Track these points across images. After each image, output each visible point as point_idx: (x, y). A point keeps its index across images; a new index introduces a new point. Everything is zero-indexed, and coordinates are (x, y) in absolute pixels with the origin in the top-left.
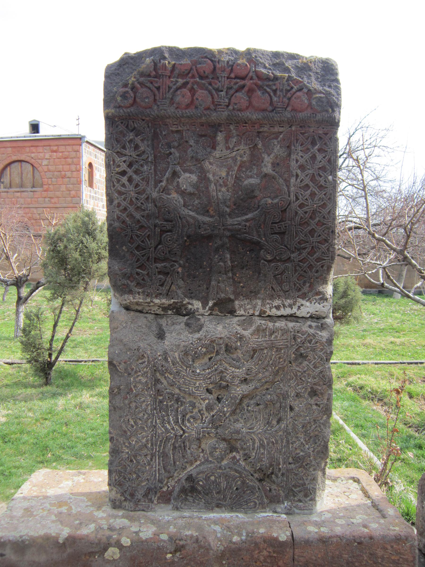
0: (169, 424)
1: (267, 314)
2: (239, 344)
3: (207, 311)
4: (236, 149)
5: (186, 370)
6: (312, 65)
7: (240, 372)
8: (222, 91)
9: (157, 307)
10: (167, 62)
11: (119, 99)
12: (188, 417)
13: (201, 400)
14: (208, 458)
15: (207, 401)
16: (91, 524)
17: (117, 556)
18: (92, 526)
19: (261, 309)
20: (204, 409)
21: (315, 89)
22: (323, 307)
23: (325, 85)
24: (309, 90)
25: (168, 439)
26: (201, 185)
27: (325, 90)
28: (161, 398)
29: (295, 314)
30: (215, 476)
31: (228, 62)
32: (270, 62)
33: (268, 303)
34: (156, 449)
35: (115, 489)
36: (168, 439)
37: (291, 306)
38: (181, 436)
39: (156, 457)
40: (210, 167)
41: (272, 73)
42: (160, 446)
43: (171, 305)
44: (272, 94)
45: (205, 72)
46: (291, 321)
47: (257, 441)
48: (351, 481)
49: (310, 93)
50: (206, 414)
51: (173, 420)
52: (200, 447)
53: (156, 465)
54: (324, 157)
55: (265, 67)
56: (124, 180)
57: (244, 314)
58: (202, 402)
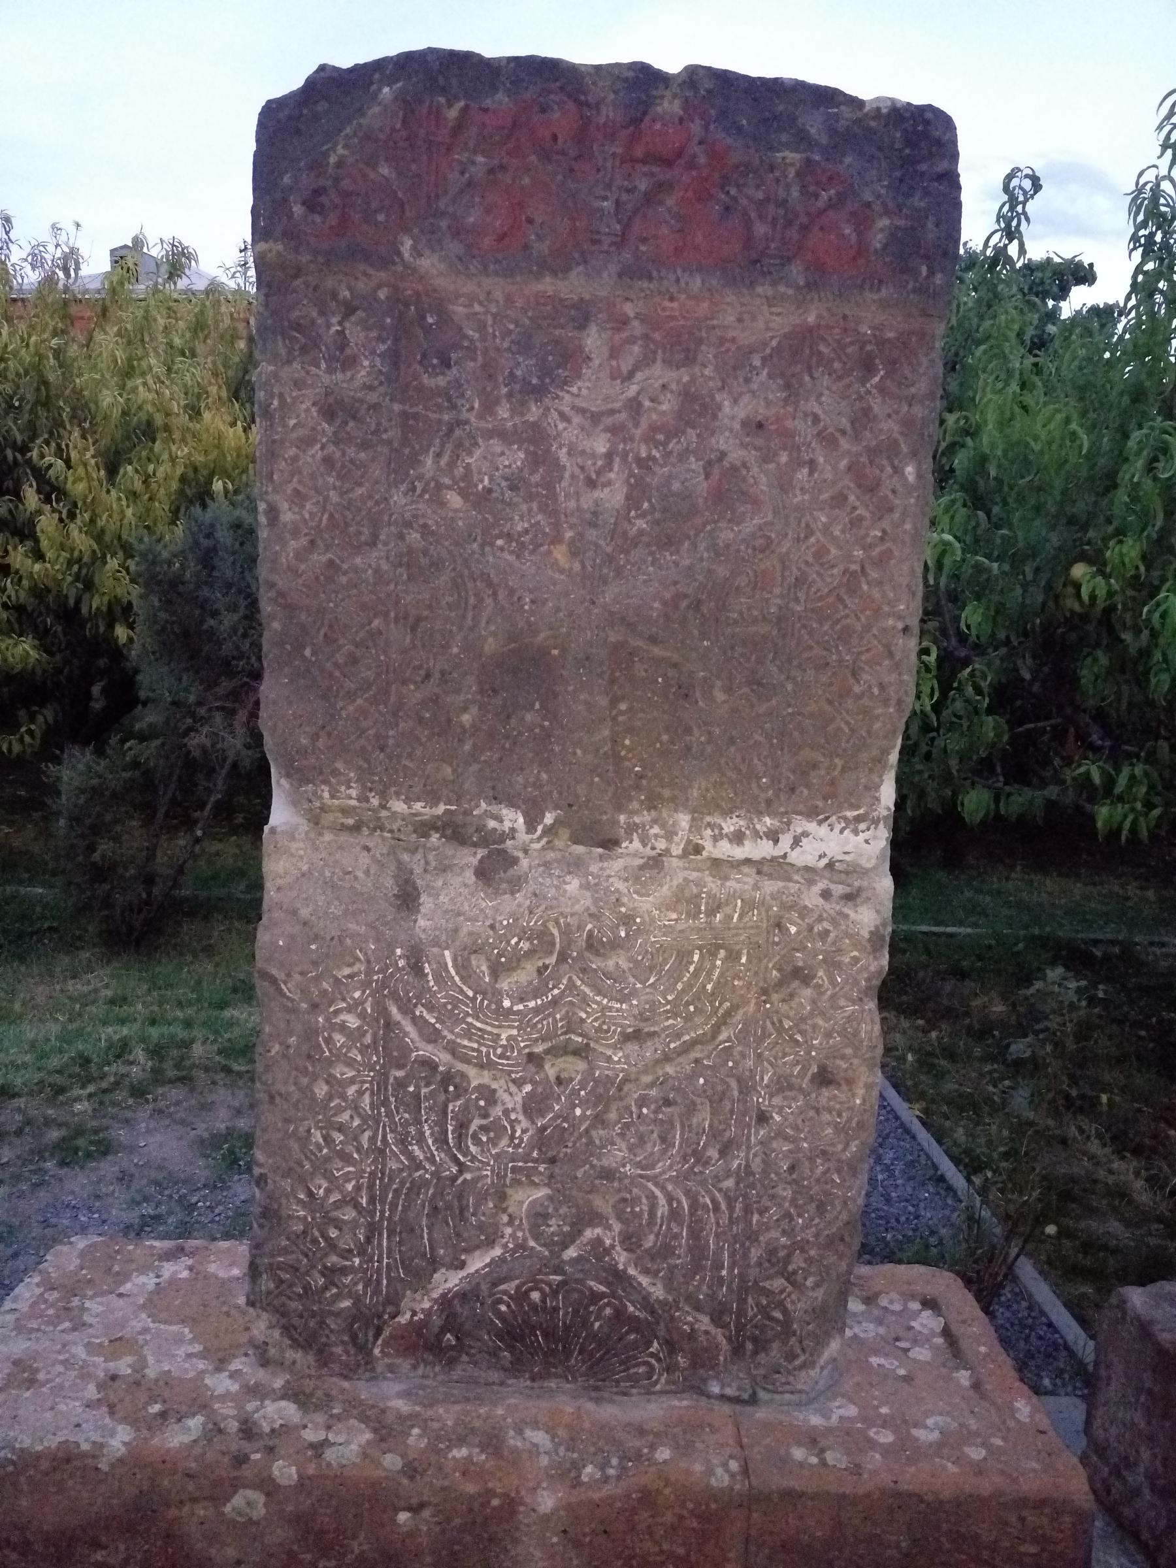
0: (421, 1148)
2: (623, 934)
3: (539, 839)
5: (474, 999)
7: (623, 1013)
9: (400, 822)
11: (298, 210)
12: (473, 1127)
14: (525, 1239)
15: (528, 1088)
16: (194, 1415)
17: (259, 1512)
18: (195, 1423)
19: (689, 842)
20: (519, 1107)
22: (867, 842)
25: (417, 1187)
26: (536, 478)
28: (400, 1074)
29: (785, 856)
30: (541, 1290)
33: (709, 824)
34: (382, 1212)
37: (774, 836)
38: (454, 1179)
39: (380, 1235)
40: (561, 426)
42: (393, 1206)
43: (438, 817)
46: (770, 876)
47: (662, 1201)
50: (525, 1124)
51: (432, 1134)
58: (513, 1089)
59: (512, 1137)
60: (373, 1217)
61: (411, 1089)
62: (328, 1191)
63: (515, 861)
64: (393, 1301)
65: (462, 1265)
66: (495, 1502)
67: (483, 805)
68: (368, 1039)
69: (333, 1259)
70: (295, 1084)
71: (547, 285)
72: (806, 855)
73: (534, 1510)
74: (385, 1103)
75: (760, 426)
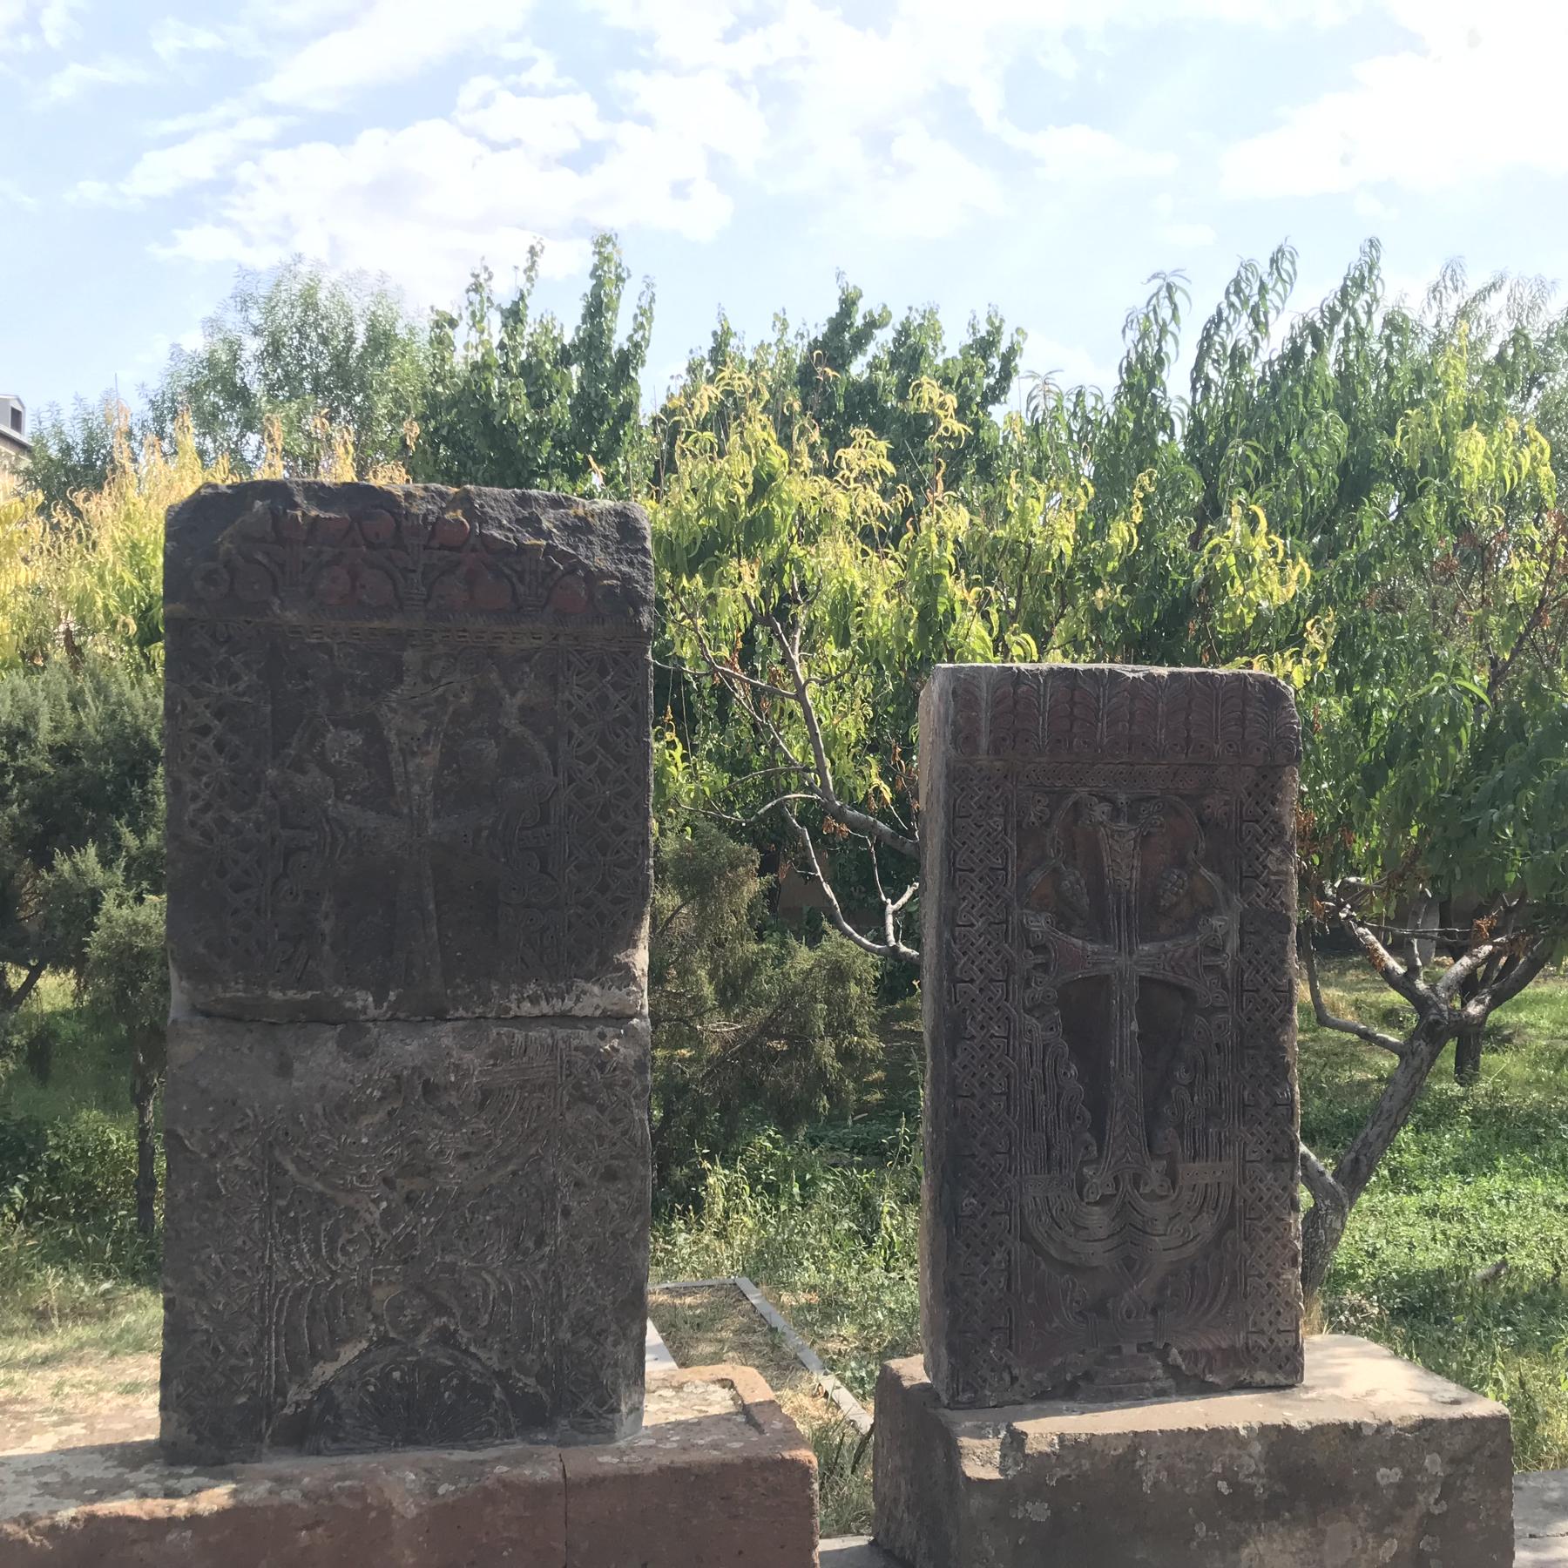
0: (301, 1261)
1: (512, 1013)
2: (453, 1079)
4: (444, 681)
6: (595, 522)
8: (414, 571)
10: (299, 513)
11: (198, 584)
13: (371, 1205)
14: (386, 1332)
21: (601, 570)
23: (621, 561)
24: (588, 572)
25: (299, 1294)
27: (620, 571)
28: (282, 1203)
31: (425, 516)
32: (512, 515)
34: (271, 1318)
35: (175, 1416)
36: (299, 1294)
38: (328, 1284)
39: (270, 1338)
40: (390, 715)
41: (515, 539)
44: (515, 580)
45: (377, 535)
47: (493, 1286)
48: (717, 1387)
49: (592, 577)
52: (368, 1309)
53: (270, 1355)
54: (624, 698)
55: (501, 527)
56: (207, 744)
57: (465, 1015)
58: (372, 1207)
59: (373, 1247)
60: (264, 1323)
61: (292, 1214)
62: (226, 1305)
63: (368, 1031)
64: (281, 1391)
65: (336, 1358)
66: (373, 1514)
67: (341, 990)
68: (257, 1175)
69: (233, 1361)
70: (198, 1220)
71: (376, 624)
72: (585, 1008)
73: (403, 1517)
74: (271, 1228)
75: (532, 709)
